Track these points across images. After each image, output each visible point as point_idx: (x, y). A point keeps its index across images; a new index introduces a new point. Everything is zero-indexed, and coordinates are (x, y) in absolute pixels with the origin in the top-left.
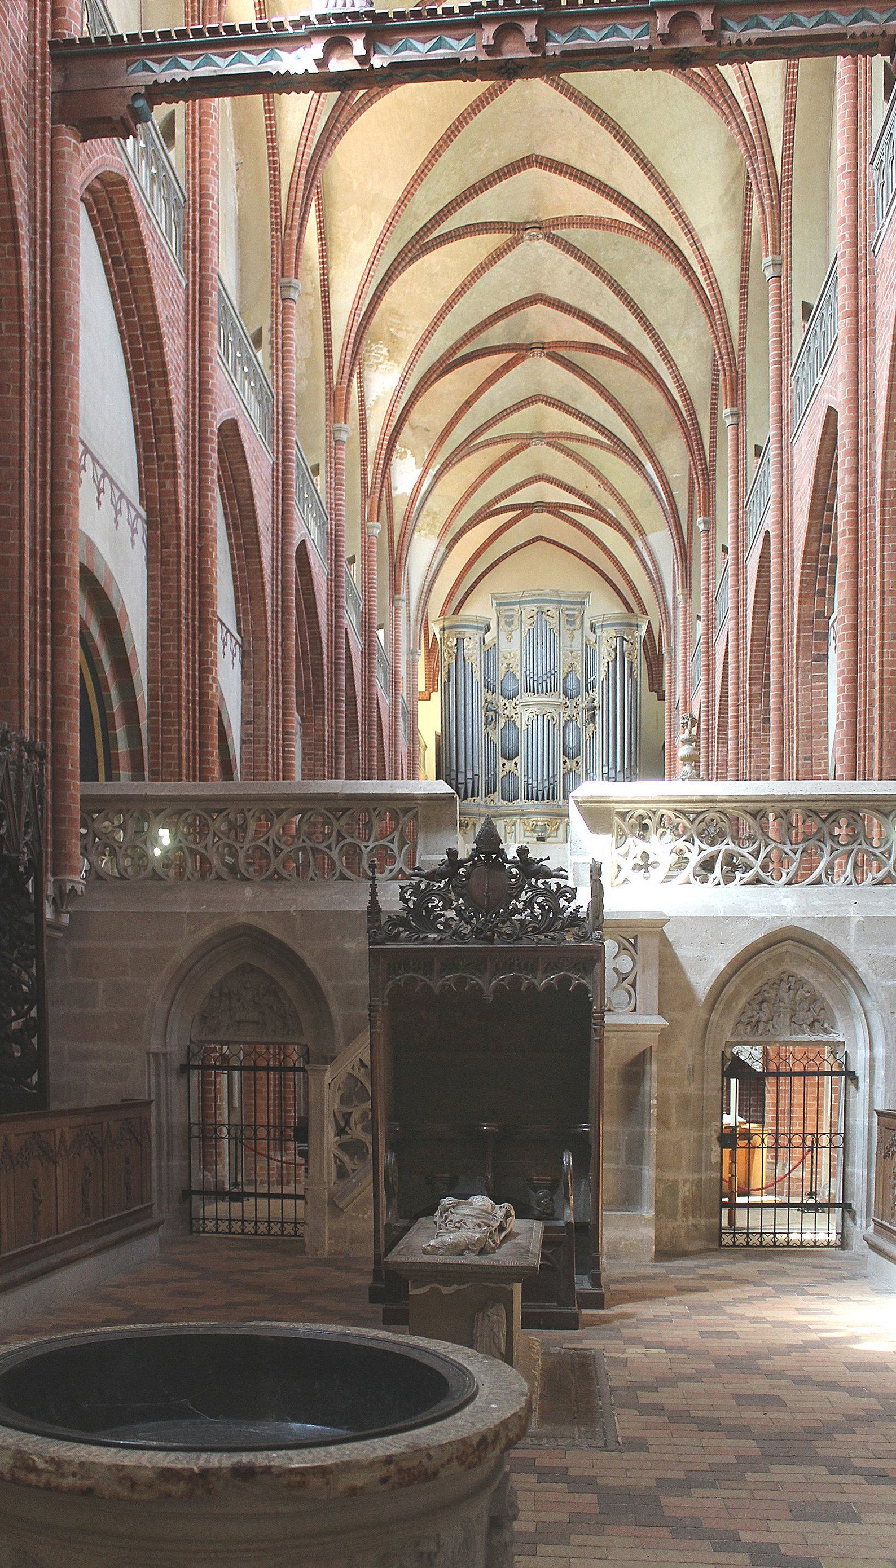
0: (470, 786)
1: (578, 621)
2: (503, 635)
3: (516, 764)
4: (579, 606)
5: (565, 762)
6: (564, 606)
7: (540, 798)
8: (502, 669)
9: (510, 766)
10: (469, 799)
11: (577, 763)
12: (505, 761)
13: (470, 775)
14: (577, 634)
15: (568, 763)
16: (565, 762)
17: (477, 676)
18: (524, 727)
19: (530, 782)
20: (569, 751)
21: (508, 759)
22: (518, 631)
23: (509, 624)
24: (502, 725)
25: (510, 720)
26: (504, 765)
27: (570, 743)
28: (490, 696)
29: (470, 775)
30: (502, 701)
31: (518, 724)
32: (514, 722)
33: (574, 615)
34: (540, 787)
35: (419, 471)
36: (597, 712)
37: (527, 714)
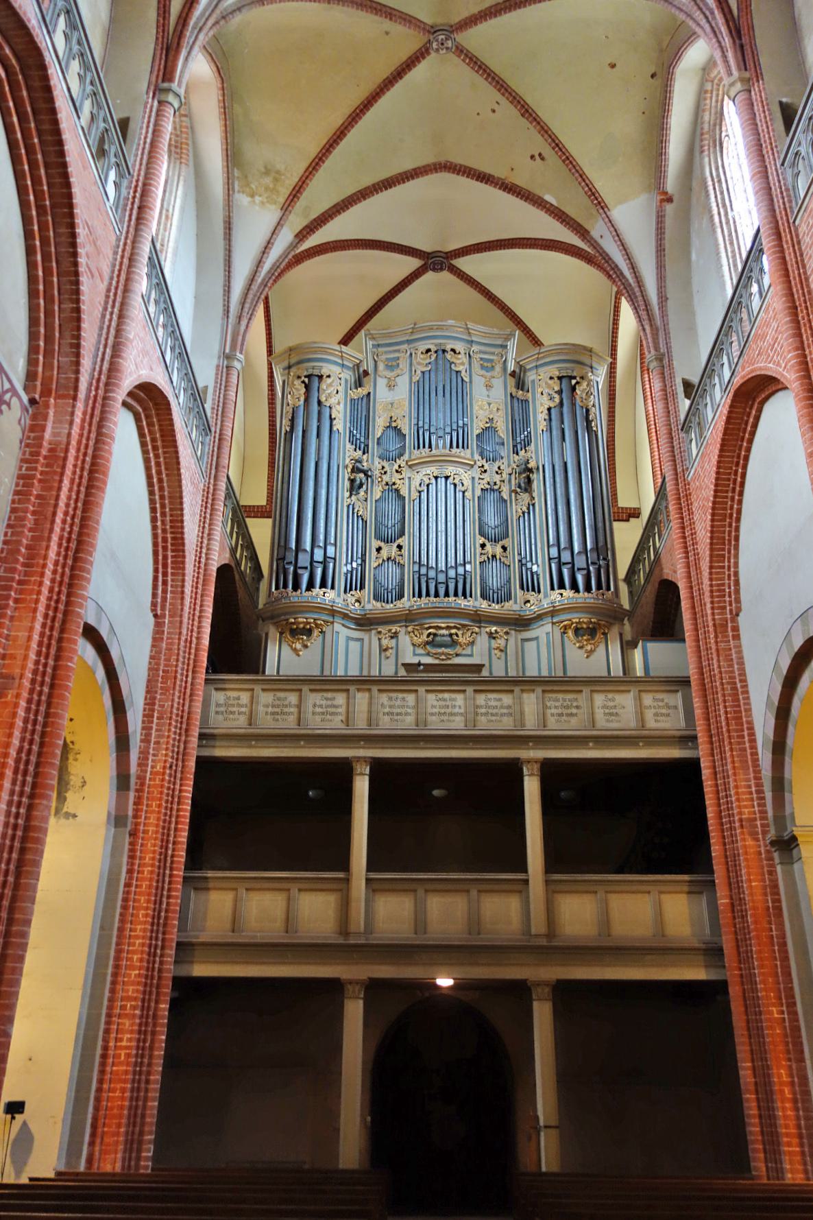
0: (319, 572)
3: (400, 547)
4: (500, 350)
5: (483, 546)
6: (475, 348)
7: (442, 591)
9: (389, 550)
10: (317, 591)
11: (504, 548)
12: (382, 544)
13: (319, 555)
14: (498, 383)
15: (489, 547)
16: (483, 546)
17: (339, 425)
18: (415, 495)
19: (423, 571)
20: (491, 532)
21: (388, 541)
22: (406, 377)
24: (377, 495)
26: (379, 550)
29: (319, 555)
30: (377, 464)
31: (404, 492)
32: (397, 491)
33: (491, 361)
34: (442, 578)
36: (534, 477)
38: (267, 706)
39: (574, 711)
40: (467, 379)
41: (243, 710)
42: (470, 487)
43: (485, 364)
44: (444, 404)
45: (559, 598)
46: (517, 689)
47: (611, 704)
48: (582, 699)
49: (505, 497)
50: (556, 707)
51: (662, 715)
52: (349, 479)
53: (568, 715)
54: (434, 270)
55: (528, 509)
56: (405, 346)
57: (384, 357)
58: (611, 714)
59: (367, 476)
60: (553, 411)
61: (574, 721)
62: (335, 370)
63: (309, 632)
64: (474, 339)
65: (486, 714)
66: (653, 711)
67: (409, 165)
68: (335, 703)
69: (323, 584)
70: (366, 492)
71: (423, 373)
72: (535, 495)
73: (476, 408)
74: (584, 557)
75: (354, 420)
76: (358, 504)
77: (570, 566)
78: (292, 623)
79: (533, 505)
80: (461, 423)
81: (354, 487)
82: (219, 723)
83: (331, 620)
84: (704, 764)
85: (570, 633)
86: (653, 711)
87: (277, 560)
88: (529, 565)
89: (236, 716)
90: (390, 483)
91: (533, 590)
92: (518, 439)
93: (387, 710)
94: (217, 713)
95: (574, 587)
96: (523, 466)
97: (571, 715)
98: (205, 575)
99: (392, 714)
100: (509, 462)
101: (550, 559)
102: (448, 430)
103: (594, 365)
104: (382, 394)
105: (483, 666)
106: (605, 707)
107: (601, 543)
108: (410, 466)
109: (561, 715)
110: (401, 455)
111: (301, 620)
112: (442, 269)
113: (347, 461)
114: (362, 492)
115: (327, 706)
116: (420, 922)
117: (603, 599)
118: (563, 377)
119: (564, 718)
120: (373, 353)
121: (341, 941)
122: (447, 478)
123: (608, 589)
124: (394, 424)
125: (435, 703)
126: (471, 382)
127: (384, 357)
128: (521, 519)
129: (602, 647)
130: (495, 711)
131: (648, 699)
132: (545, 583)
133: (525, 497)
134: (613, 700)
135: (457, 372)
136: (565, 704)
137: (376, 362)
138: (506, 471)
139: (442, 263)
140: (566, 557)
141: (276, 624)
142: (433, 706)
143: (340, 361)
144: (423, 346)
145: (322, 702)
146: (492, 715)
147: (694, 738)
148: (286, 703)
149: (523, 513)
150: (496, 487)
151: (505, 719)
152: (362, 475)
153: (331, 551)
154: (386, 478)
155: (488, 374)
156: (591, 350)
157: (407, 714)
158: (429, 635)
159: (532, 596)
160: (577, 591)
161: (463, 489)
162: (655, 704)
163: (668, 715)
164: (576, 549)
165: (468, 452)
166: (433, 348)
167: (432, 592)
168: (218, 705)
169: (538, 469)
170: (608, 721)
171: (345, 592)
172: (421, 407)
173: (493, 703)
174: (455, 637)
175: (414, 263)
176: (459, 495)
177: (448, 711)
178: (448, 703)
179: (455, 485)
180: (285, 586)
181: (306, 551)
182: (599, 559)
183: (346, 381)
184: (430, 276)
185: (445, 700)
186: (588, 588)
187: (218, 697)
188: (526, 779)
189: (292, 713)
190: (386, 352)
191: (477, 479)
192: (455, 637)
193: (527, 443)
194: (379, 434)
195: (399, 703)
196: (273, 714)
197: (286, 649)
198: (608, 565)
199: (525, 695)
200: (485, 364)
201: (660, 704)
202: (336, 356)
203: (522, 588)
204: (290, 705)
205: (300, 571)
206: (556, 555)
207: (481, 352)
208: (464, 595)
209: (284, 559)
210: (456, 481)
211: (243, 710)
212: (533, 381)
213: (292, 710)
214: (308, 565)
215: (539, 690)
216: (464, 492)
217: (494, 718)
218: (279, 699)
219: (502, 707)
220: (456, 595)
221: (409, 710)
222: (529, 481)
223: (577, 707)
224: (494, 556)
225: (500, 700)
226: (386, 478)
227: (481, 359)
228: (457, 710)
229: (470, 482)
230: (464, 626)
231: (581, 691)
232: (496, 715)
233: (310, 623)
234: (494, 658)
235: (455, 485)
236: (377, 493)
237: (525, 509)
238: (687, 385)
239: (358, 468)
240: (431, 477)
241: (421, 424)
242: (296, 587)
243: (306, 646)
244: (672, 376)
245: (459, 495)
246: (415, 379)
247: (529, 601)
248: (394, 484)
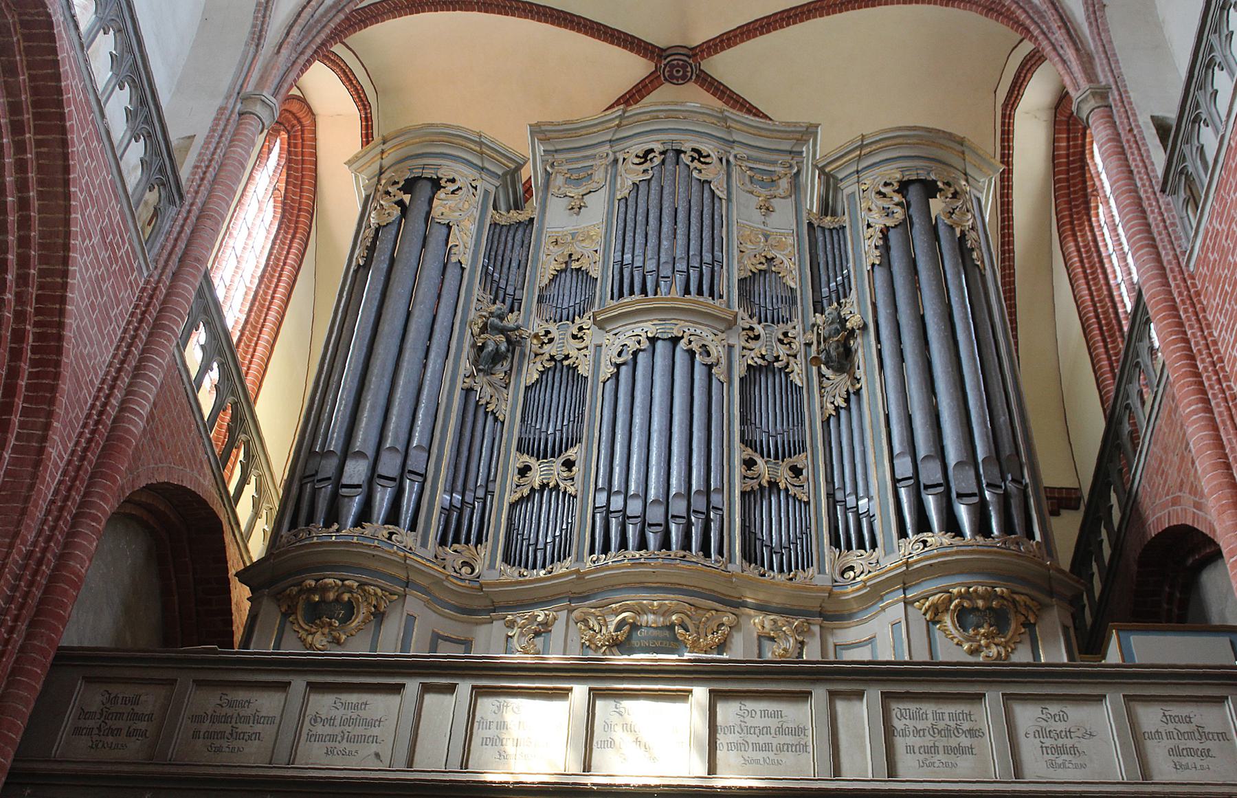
1: (784, 184)
5: (749, 463)
6: (737, 150)
10: (377, 528)
12: (532, 461)
21: (542, 455)
22: (603, 194)
26: (524, 471)
29: (390, 465)
34: (655, 514)
39: (965, 741)
41: (142, 725)
42: (723, 361)
47: (1060, 726)
50: (917, 732)
51: (1191, 752)
52: (474, 345)
53: (949, 750)
55: (847, 400)
56: (606, 148)
60: (892, 235)
62: (464, 175)
66: (1170, 743)
74: (972, 473)
78: (313, 590)
79: (858, 393)
85: (948, 620)
88: (851, 501)
90: (558, 358)
91: (861, 546)
92: (825, 290)
94: (77, 731)
95: (951, 525)
97: (959, 750)
101: (895, 481)
103: (969, 171)
106: (1040, 733)
107: (1007, 450)
118: (910, 182)
122: (675, 341)
123: (1031, 536)
124: (575, 265)
126: (729, 200)
128: (833, 422)
132: (885, 526)
133: (839, 383)
134: (1063, 718)
136: (941, 725)
137: (548, 174)
140: (930, 473)
143: (477, 162)
144: (640, 149)
145: (334, 713)
149: (837, 409)
156: (961, 142)
158: (619, 627)
159: (856, 558)
161: (708, 361)
162: (1170, 727)
163: (1206, 753)
164: (952, 457)
166: (658, 147)
168: (84, 714)
169: (864, 327)
170: (1052, 764)
171: (443, 542)
172: (629, 234)
179: (692, 354)
182: (1004, 479)
183: (486, 192)
184: (665, 94)
186: (982, 527)
190: (568, 161)
193: (844, 290)
199: (841, 706)
201: (1184, 728)
203: (835, 542)
204: (257, 718)
206: (909, 473)
208: (705, 548)
210: (694, 346)
211: (142, 725)
215: (874, 694)
216: (710, 367)
218: (230, 704)
222: (847, 354)
223: (972, 733)
224: (773, 485)
231: (980, 697)
233: (350, 590)
235: (692, 354)
237: (840, 402)
238: (1163, 129)
240: (643, 339)
241: (628, 257)
244: (1129, 114)
247: (852, 568)
248: (567, 357)
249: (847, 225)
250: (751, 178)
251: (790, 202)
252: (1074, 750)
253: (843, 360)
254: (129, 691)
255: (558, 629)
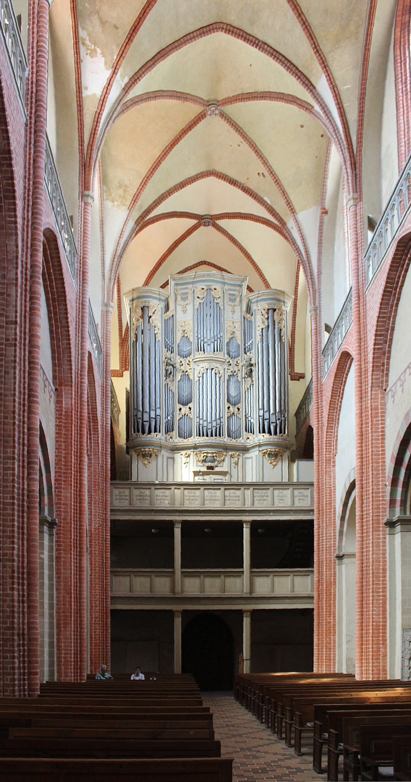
1: (238, 299)
2: (179, 308)
6: (227, 287)
8: (179, 335)
10: (153, 433)
13: (153, 415)
14: (237, 309)
18: (197, 379)
23: (184, 299)
25: (185, 374)
27: (233, 393)
28: (169, 354)
31: (191, 377)
33: (234, 295)
35: (109, 73)
36: (253, 368)
37: (199, 368)
38: (136, 496)
39: (266, 498)
40: (222, 308)
41: (127, 497)
43: (231, 297)
44: (210, 323)
45: (262, 438)
46: (242, 488)
47: (281, 495)
48: (269, 492)
49: (240, 380)
50: (258, 496)
51: (302, 500)
54: (205, 225)
57: (180, 292)
58: (281, 500)
59: (174, 367)
61: (265, 502)
63: (151, 456)
64: (226, 281)
65: (229, 500)
66: (298, 498)
67: (193, 173)
68: (165, 494)
69: (155, 431)
70: (173, 376)
71: (200, 303)
72: (254, 379)
73: (226, 326)
74: (275, 416)
75: (166, 335)
76: (169, 383)
77: (268, 420)
80: (219, 336)
81: (168, 374)
82: (118, 504)
83: (160, 449)
84: (315, 523)
86: (298, 498)
87: (134, 416)
89: (124, 501)
90: (185, 371)
93: (187, 498)
94: (116, 499)
96: (248, 363)
97: (264, 500)
98: (106, 432)
99: (190, 500)
100: (242, 360)
102: (213, 341)
104: (180, 317)
105: (228, 472)
106: (278, 496)
108: (195, 362)
109: (260, 500)
110: (189, 355)
111: (147, 449)
112: (209, 225)
113: (164, 358)
114: (171, 377)
115: (162, 496)
116: (202, 588)
117: (282, 439)
119: (262, 501)
120: (175, 289)
121: (172, 596)
122: (212, 369)
124: (186, 335)
125: (208, 495)
126: (224, 309)
127: (180, 292)
129: (280, 462)
130: (233, 498)
131: (296, 492)
134: (282, 493)
135: (217, 303)
138: (241, 365)
139: (209, 222)
141: (136, 451)
142: (207, 496)
146: (232, 500)
147: (312, 511)
148: (145, 494)
150: (235, 374)
151: (237, 502)
152: (171, 367)
153: (158, 413)
154: (182, 368)
155: (233, 304)
157: (196, 500)
160: (271, 434)
161: (220, 375)
163: (304, 500)
164: (272, 412)
165: (222, 353)
167: (205, 434)
168: (116, 495)
170: (279, 503)
173: (232, 495)
174: (215, 458)
175: (193, 222)
176: (218, 379)
177: (213, 498)
178: (213, 495)
180: (138, 432)
181: (146, 412)
185: (212, 493)
187: (116, 492)
188: (244, 529)
189: (147, 500)
191: (226, 370)
192: (215, 458)
194: (178, 342)
195: (192, 495)
196: (140, 499)
197: (140, 464)
198: (285, 420)
199: (246, 491)
200: (231, 297)
201: (301, 495)
202: (156, 294)
204: (146, 496)
205: (145, 423)
207: (230, 290)
209: (137, 416)
210: (216, 372)
211: (127, 497)
212: (255, 310)
213: (147, 498)
214: (148, 420)
215: (251, 488)
217: (232, 501)
218: (141, 492)
219: (236, 497)
220: (216, 436)
221: (197, 498)
223: (267, 496)
225: (235, 493)
226: (182, 368)
227: (229, 294)
228: (217, 498)
229: (223, 371)
230: (220, 452)
231: (269, 489)
232: (233, 500)
234: (232, 468)
236: (178, 377)
239: (169, 364)
240: (205, 369)
241: (199, 337)
242: (143, 433)
243: (149, 462)
245: (218, 379)
246: (196, 307)
248: (187, 372)
249: (253, 321)
250: (230, 298)
251: (239, 307)
252: (283, 500)
253: (250, 374)
254: (123, 490)
255: (191, 456)
